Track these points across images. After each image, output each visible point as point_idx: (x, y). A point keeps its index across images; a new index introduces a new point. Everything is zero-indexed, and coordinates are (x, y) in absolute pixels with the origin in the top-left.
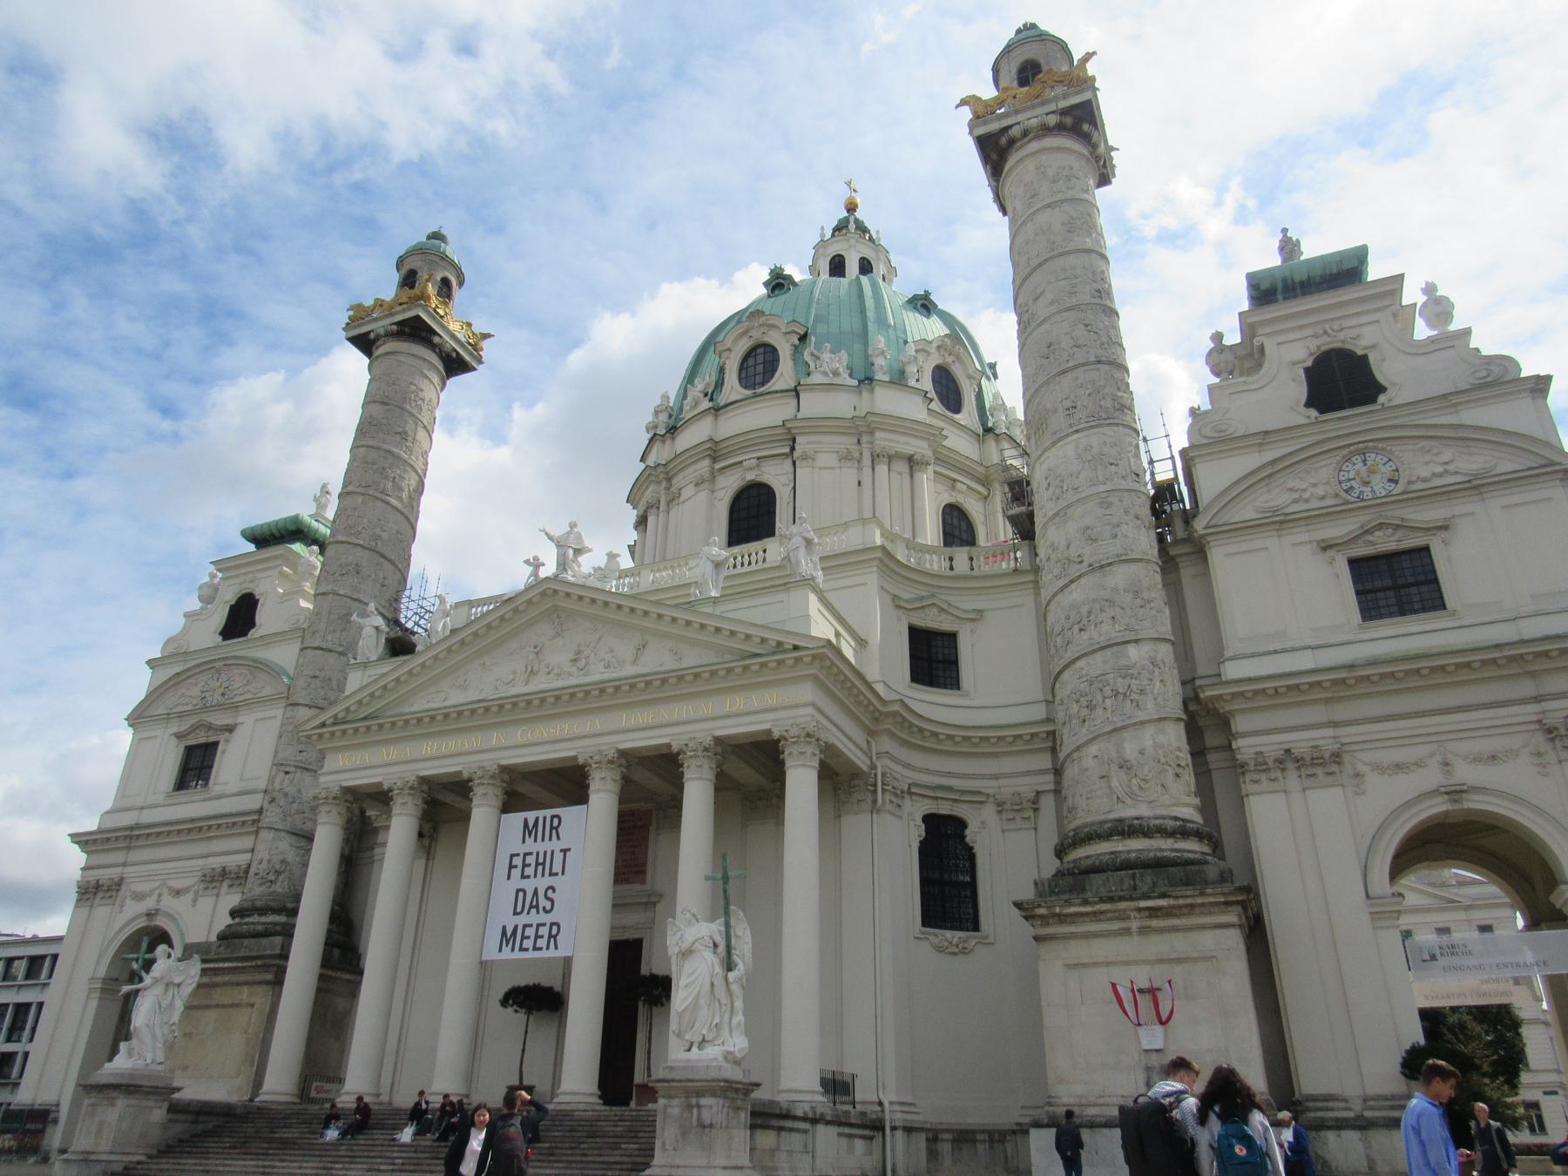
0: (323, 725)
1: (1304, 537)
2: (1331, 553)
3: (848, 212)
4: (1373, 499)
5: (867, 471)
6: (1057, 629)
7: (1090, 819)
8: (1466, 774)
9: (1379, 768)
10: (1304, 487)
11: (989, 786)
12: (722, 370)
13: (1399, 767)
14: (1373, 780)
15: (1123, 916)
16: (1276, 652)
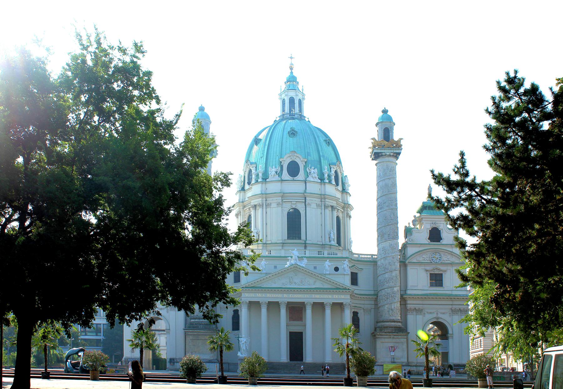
0: (243, 287)
1: (423, 268)
2: (428, 272)
3: (291, 69)
4: (436, 263)
5: (323, 210)
6: (382, 281)
7: (385, 318)
8: (440, 315)
9: (428, 313)
10: (425, 257)
11: (362, 306)
12: (282, 167)
13: (431, 313)
14: (426, 314)
15: (390, 335)
16: (416, 290)
